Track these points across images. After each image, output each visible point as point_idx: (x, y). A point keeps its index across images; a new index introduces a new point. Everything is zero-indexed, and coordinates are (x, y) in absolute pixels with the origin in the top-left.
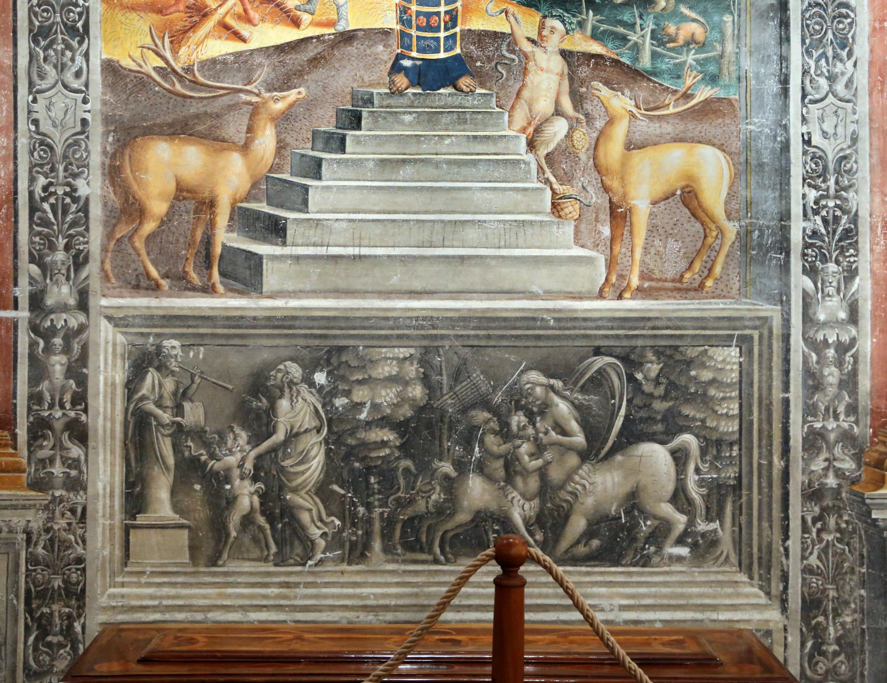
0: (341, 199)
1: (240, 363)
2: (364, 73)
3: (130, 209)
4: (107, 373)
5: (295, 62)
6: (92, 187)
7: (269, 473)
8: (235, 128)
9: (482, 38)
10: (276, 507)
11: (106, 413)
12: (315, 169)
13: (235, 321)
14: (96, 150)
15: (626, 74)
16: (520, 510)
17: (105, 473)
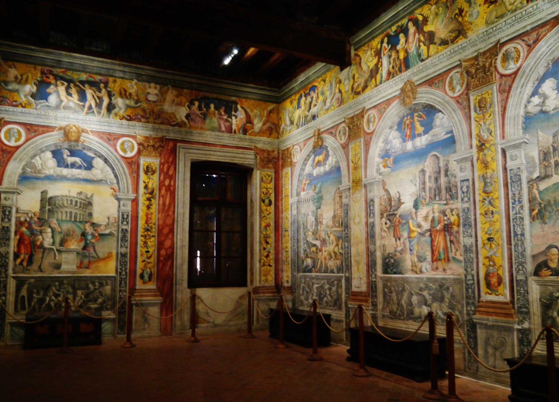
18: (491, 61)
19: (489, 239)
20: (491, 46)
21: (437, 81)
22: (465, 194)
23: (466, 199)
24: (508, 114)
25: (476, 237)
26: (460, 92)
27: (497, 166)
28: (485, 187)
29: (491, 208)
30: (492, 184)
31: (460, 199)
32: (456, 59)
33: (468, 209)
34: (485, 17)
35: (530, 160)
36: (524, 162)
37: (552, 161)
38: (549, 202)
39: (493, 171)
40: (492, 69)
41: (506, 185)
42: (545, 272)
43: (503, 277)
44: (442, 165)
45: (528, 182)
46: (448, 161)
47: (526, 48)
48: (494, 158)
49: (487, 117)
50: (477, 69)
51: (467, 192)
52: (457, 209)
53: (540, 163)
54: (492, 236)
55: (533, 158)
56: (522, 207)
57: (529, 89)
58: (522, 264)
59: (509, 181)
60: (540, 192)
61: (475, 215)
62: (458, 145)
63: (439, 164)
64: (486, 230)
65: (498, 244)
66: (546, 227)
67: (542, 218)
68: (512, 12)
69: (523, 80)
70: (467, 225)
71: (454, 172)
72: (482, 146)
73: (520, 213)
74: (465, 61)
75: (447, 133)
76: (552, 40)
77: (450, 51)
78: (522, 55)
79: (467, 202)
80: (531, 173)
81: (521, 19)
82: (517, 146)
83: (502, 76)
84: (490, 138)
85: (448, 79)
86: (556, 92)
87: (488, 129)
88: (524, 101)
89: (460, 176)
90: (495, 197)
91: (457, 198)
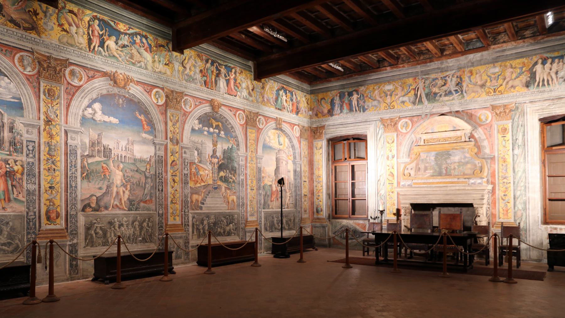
0: (209, 201)
1: (201, 217)
2: (210, 188)
3: (192, 202)
4: (190, 219)
5: (205, 186)
6: (189, 199)
7: (203, 229)
8: (200, 193)
9: (219, 185)
10: (204, 233)
11: (190, 223)
12: (206, 198)
13: (200, 213)
14: (189, 195)
15: (229, 189)
16: (222, 231)
17: (191, 230)
18: (61, 69)
19: (50, 187)
20: (62, 58)
21: (4, 49)
22: (31, 152)
23: (31, 155)
24: (71, 109)
25: (39, 184)
26: (31, 73)
27: (60, 139)
28: (49, 151)
29: (54, 167)
30: (55, 151)
31: (25, 154)
32: (28, 46)
33: (33, 163)
34: (59, 35)
35: (83, 144)
36: (80, 143)
37: (96, 148)
38: (93, 170)
39: (57, 142)
40: (61, 74)
41: (66, 154)
42: (88, 209)
43: (61, 213)
44: (5, 121)
45: (81, 156)
46: (14, 121)
47: (86, 78)
48: (59, 134)
49: (55, 104)
50: (48, 67)
51: (33, 151)
52: (22, 161)
53: (89, 148)
54: (53, 185)
55: (85, 143)
56: (76, 170)
57: (86, 102)
58: (75, 205)
59: (69, 152)
60: (88, 164)
61: (39, 168)
62: (26, 113)
63: (2, 119)
64: (48, 181)
65: (58, 192)
66: (90, 184)
67: (88, 179)
68: (79, 48)
69: (83, 94)
70: (31, 174)
71: (21, 132)
72: (48, 122)
73: (75, 173)
74: (37, 53)
75: (13, 98)
76: (101, 83)
77: (22, 35)
78: (83, 79)
79: (31, 158)
80: (84, 151)
81: (84, 57)
82: (76, 132)
83: (69, 83)
84: (56, 119)
85: (18, 56)
86: (101, 112)
87: (55, 113)
88: (83, 107)
89: (26, 136)
90: (57, 160)
91: (22, 153)
